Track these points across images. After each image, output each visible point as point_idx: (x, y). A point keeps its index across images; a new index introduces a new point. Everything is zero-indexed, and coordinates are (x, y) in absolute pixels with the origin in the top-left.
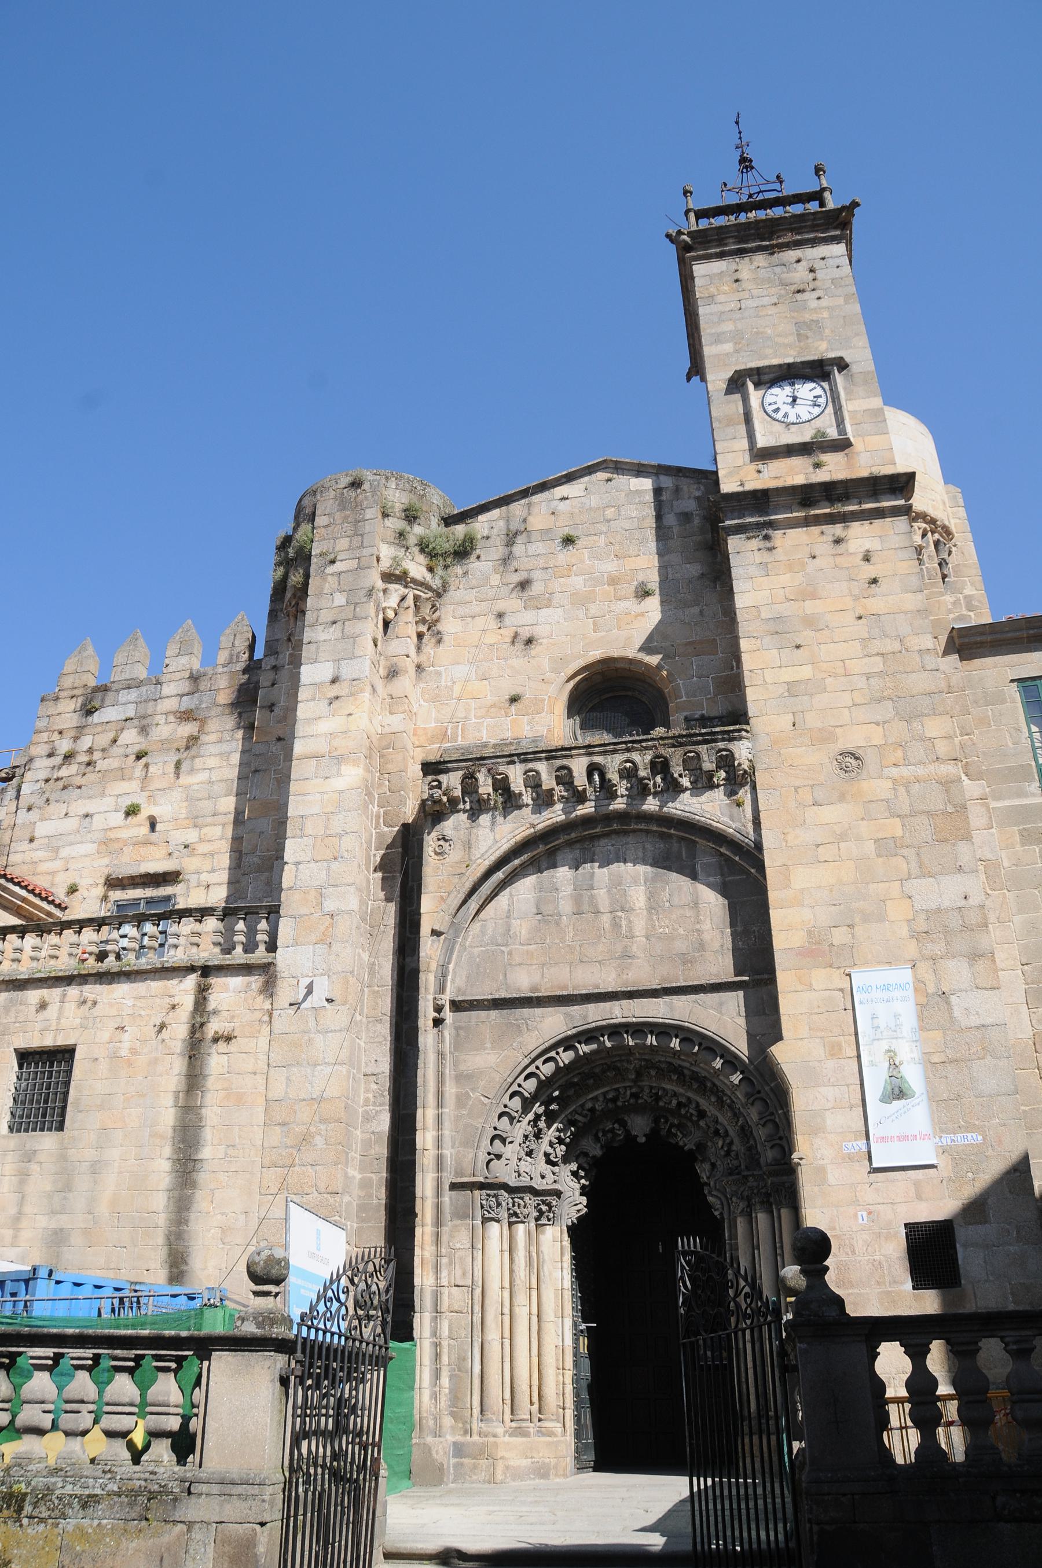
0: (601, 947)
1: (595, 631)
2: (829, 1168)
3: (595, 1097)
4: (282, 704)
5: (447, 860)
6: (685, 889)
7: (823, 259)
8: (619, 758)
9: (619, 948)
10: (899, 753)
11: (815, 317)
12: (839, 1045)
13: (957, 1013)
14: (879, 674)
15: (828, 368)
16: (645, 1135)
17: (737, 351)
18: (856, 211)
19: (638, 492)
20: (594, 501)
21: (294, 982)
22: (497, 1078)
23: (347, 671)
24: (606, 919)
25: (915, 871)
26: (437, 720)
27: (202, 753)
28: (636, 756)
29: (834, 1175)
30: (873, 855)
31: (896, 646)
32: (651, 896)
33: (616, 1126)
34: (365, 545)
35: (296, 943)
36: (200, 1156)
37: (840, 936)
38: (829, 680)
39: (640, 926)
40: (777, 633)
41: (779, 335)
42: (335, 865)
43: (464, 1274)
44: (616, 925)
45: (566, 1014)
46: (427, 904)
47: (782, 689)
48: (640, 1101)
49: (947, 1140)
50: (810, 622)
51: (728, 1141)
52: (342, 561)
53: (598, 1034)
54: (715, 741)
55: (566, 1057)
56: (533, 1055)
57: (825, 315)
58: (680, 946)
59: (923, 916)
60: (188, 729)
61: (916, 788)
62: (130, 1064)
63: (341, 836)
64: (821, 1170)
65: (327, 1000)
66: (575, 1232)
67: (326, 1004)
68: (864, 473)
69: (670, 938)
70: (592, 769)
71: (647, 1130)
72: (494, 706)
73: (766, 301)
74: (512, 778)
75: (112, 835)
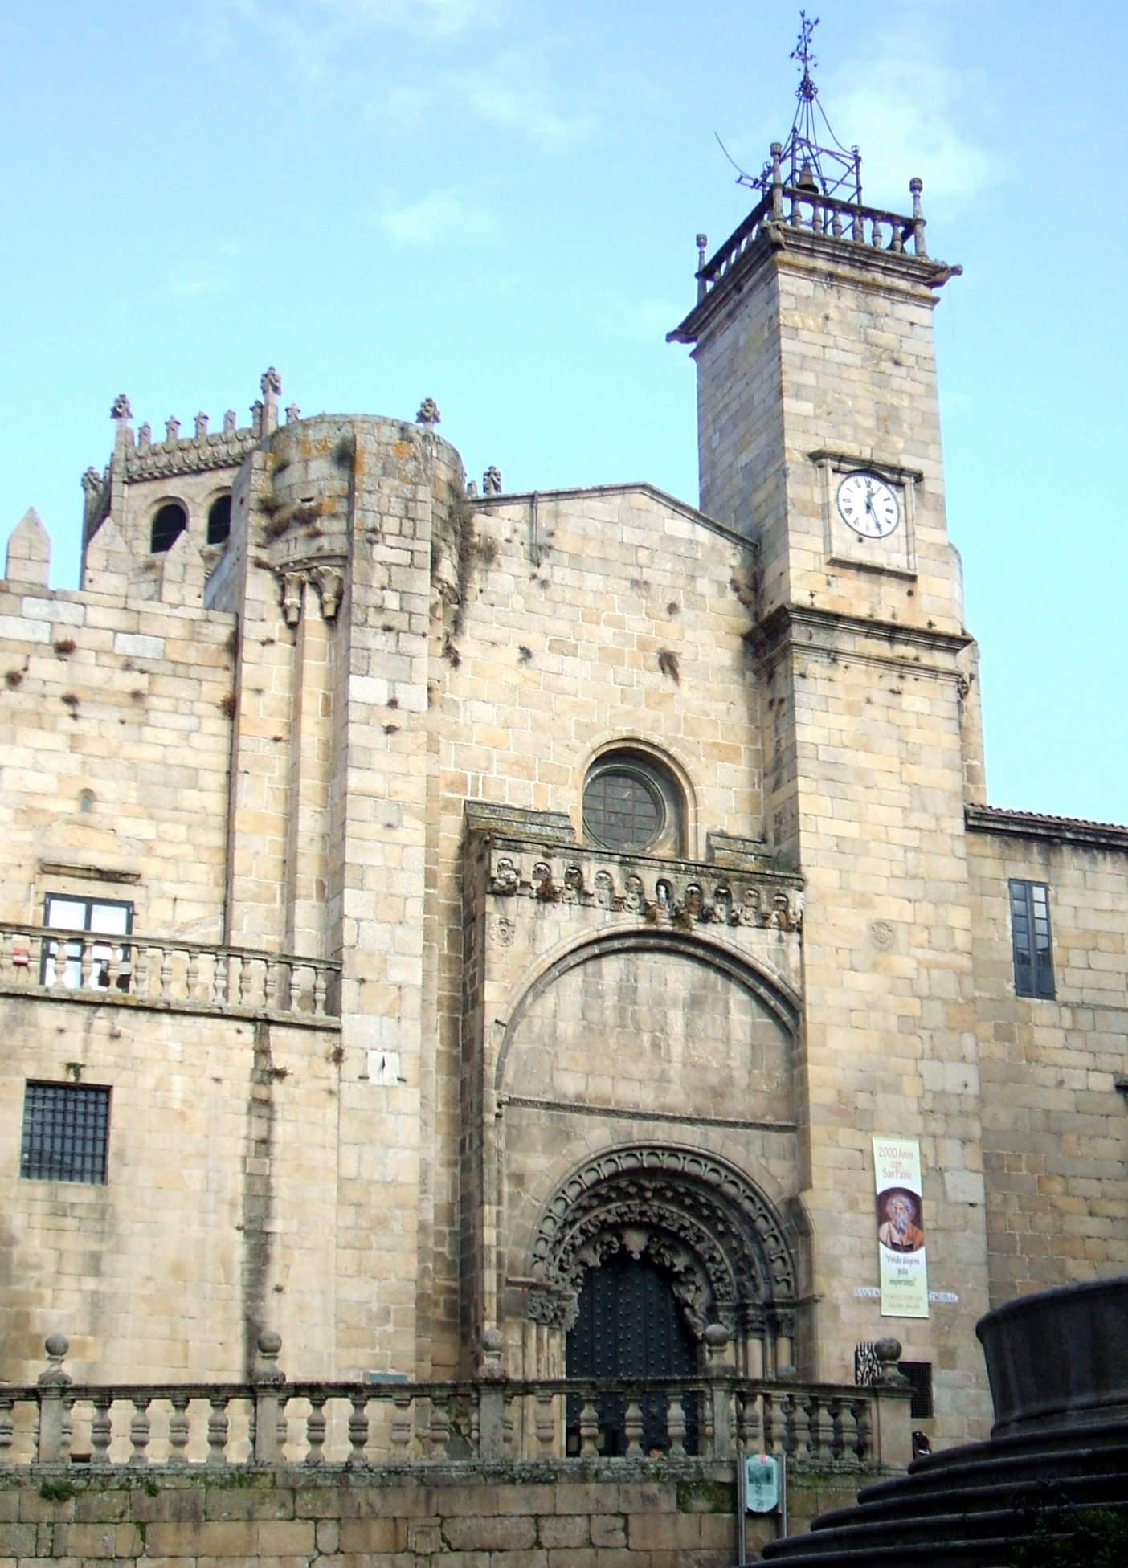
0: (642, 1066)
1: (622, 703)
2: (843, 1308)
3: (608, 1214)
4: (273, 691)
5: (510, 949)
6: (719, 1022)
7: (912, 324)
8: (688, 879)
9: (657, 1068)
10: (925, 935)
11: (895, 401)
12: (857, 1203)
13: (949, 1188)
14: (917, 849)
15: (905, 479)
16: (641, 1253)
17: (816, 417)
18: (953, 280)
19: (672, 539)
20: (630, 536)
21: (362, 1054)
22: (548, 1183)
23: (403, 694)
24: (646, 1038)
25: (928, 1053)
26: (457, 765)
27: (152, 721)
28: (704, 885)
29: (846, 1314)
30: (894, 1028)
31: (932, 824)
32: (688, 1024)
33: (615, 1239)
34: (418, 535)
35: (360, 1010)
36: (269, 1229)
37: (863, 1100)
38: (872, 845)
39: (677, 1049)
40: (831, 780)
41: (858, 412)
42: (400, 931)
43: (516, 1369)
44: (656, 1046)
45: (614, 1131)
46: (491, 992)
47: (832, 842)
48: (646, 1220)
49: (933, 1296)
50: (861, 775)
51: (723, 1267)
52: (392, 548)
53: (637, 1153)
54: (773, 884)
55: (607, 1170)
56: (581, 1164)
57: (906, 403)
58: (713, 1079)
59: (929, 1096)
60: (138, 681)
61: (935, 973)
62: (182, 1116)
63: (406, 899)
64: (835, 1308)
65: (399, 1079)
66: (569, 1336)
67: (397, 1083)
68: (922, 625)
69: (704, 1068)
70: (661, 882)
71: (643, 1248)
72: (516, 763)
73: (849, 358)
74: (585, 874)
75: (36, 803)
